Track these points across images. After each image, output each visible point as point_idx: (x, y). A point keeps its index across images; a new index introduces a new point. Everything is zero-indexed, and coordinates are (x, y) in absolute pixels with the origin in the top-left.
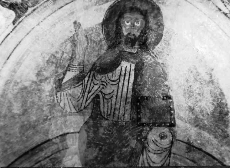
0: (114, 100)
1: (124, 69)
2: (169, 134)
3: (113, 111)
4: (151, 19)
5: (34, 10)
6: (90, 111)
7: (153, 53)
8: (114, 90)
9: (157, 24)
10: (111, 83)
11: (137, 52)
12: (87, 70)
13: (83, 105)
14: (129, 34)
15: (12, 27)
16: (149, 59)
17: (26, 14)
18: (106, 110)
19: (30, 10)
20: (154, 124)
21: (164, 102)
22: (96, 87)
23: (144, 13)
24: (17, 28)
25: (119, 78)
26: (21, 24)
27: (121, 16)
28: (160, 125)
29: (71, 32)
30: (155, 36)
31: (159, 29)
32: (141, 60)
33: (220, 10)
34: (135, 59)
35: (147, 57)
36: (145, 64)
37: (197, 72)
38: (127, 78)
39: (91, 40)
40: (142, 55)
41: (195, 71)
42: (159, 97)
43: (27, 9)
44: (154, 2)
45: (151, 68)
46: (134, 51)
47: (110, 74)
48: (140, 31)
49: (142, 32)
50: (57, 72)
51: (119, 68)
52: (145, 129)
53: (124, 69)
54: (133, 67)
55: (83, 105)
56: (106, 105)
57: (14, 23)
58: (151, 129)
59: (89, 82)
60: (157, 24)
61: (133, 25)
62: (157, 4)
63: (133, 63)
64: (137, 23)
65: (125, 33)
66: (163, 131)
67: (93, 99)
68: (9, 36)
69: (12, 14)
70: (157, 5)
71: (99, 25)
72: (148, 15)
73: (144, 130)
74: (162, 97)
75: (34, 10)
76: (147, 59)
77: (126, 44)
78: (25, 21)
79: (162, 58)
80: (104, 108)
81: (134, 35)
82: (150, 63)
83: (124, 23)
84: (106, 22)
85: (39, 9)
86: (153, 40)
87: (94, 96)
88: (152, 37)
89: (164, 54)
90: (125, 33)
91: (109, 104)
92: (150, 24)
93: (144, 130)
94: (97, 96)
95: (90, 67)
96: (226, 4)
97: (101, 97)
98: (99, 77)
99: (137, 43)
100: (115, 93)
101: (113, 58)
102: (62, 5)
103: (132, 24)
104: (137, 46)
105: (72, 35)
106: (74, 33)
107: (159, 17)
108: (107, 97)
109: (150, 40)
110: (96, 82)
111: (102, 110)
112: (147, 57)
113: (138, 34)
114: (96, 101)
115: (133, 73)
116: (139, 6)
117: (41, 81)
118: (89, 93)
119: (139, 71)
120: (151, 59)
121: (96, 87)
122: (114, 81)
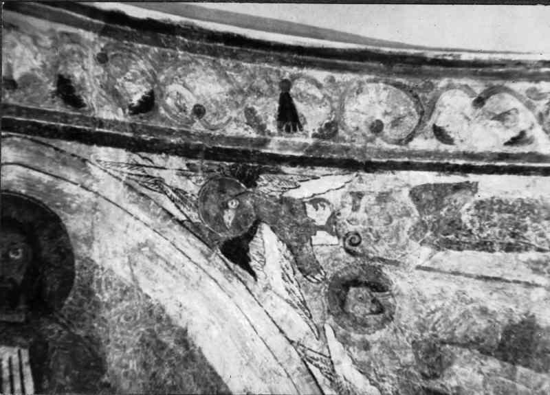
4: (43, 242)
7: (62, 316)
9: (58, 251)
11: (27, 321)
16: (56, 331)
30: (58, 278)
31: (65, 261)
32: (40, 336)
33: (170, 215)
34: (26, 337)
35: (50, 327)
36: (51, 345)
38: (17, 386)
40: (39, 324)
41: (154, 341)
44: (44, 205)
45: (67, 352)
48: (24, 270)
49: (27, 274)
54: (25, 353)
62: (52, 209)
63: (24, 347)
64: (14, 253)
70: (53, 212)
76: (51, 332)
79: (83, 325)
81: (11, 280)
82: (59, 340)
86: (56, 287)
88: (52, 283)
89: (85, 315)
92: (44, 253)
96: (180, 205)
99: (22, 299)
104: (22, 307)
107: (60, 235)
109: (49, 289)
112: (50, 327)
115: (27, 370)
116: (14, 214)
120: (60, 332)
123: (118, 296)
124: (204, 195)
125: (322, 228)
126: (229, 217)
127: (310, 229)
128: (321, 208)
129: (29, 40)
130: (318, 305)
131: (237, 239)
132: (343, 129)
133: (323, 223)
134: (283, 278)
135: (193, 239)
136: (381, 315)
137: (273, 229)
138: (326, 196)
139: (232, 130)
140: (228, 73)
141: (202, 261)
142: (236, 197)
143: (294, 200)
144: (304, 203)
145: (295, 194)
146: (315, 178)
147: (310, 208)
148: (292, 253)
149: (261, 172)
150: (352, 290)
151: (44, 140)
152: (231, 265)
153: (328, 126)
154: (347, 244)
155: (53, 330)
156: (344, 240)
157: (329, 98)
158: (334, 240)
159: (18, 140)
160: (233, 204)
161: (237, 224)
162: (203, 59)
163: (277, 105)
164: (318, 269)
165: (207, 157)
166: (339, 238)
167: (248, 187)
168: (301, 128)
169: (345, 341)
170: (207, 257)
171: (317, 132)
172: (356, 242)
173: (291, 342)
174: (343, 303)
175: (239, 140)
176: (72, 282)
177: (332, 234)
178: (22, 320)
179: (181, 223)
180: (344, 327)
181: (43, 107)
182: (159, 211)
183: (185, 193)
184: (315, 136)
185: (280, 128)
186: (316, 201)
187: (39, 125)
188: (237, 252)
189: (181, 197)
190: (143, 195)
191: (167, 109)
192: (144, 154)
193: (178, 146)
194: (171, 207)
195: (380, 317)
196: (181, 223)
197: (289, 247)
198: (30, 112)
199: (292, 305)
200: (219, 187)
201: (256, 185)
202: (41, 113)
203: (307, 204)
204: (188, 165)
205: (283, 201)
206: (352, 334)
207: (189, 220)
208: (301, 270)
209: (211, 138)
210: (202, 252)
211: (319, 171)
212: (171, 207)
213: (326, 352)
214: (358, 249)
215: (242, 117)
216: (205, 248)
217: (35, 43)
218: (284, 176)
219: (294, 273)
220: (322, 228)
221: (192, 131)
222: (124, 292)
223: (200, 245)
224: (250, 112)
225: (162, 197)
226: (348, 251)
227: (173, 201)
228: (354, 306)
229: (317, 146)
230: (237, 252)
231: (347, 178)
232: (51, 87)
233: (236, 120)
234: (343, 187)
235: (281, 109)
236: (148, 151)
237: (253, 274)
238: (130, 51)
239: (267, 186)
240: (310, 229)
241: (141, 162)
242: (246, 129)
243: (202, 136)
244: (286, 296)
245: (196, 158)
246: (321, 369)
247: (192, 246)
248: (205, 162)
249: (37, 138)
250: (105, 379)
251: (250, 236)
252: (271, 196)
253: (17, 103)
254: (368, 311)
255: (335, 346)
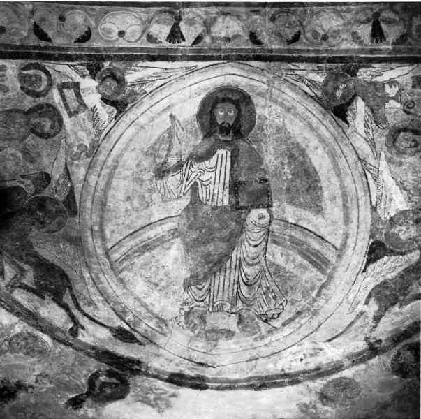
0: (212, 186)
1: (220, 156)
2: (267, 215)
3: (211, 196)
4: (243, 108)
5: (133, 105)
6: (189, 197)
8: (211, 178)
10: (209, 170)
11: (232, 140)
12: (184, 158)
13: (182, 191)
14: (223, 123)
15: (113, 121)
17: (126, 109)
18: (204, 196)
19: (129, 105)
20: (252, 207)
21: (260, 186)
22: (194, 175)
23: (236, 103)
24: (118, 123)
25: (216, 166)
26: (122, 118)
27: (214, 107)
28: (258, 207)
29: (168, 124)
33: (307, 93)
34: (230, 147)
37: (291, 153)
38: (224, 165)
39: (187, 131)
41: (288, 153)
42: (256, 180)
43: (126, 105)
46: (229, 139)
47: (207, 162)
50: (156, 162)
51: (216, 156)
52: (243, 211)
53: (220, 156)
54: (229, 153)
55: (182, 191)
56: (204, 190)
57: (115, 118)
58: (249, 211)
59: (187, 170)
60: (249, 111)
61: (226, 115)
65: (220, 123)
66: (262, 212)
67: (192, 186)
68: (112, 130)
69: (113, 110)
71: (194, 116)
72: (240, 104)
73: (242, 213)
74: (259, 181)
75: (133, 105)
76: (242, 145)
77: (221, 132)
78: (125, 116)
80: (203, 195)
83: (217, 112)
84: (200, 114)
85: (137, 105)
87: (192, 183)
88: (245, 127)
90: (220, 123)
91: (208, 190)
93: (242, 213)
94: (196, 183)
95: (187, 156)
97: (199, 184)
98: (196, 165)
99: (231, 131)
100: (213, 180)
101: (208, 147)
102: (158, 100)
103: (225, 113)
105: (168, 127)
106: (170, 125)
108: (205, 183)
110: (193, 170)
111: (201, 196)
112: (242, 143)
113: (231, 123)
114: (195, 187)
115: (229, 159)
116: (230, 96)
117: (141, 171)
118: (187, 180)
119: (235, 157)
121: (194, 175)
122: (211, 168)
123: (275, 132)
124: (326, 83)
125: (392, 98)
126: (339, 94)
127: (386, 99)
128: (393, 87)
129: (235, 18)
130: (381, 141)
131: (343, 105)
132: (410, 37)
133: (393, 95)
134: (365, 126)
135: (317, 105)
136: (415, 149)
137: (364, 100)
138: (398, 80)
139: (344, 46)
140: (342, 14)
141: (321, 117)
142: (344, 83)
143: (378, 82)
144: (384, 84)
145: (379, 79)
146: (392, 69)
147: (387, 87)
148: (373, 112)
149: (360, 67)
150: (402, 134)
151: (244, 62)
152: (336, 118)
153: (402, 36)
154: (405, 108)
155: (242, 144)
156: (404, 105)
157: (403, 19)
158: (398, 105)
159: (233, 64)
160: (342, 87)
161: (343, 97)
162: (328, 9)
163: (371, 28)
164: (385, 121)
165: (328, 62)
166: (401, 104)
167: (352, 76)
168: (385, 40)
169: (389, 161)
170: (324, 114)
171: (395, 41)
172: (411, 106)
173: (360, 159)
174: (395, 140)
175: (347, 51)
176: (254, 126)
177: (398, 102)
178: (230, 139)
179: (312, 97)
180: (391, 154)
181: (243, 47)
182: (300, 91)
183: (315, 82)
184: (393, 43)
185: (372, 41)
186: (392, 83)
187: (241, 56)
188: (340, 112)
189: (312, 84)
190: (293, 84)
191: (307, 39)
192: (294, 64)
193: (313, 57)
194: (307, 89)
195: (413, 149)
196: (312, 97)
197: (372, 110)
198: (237, 50)
199: (367, 141)
200: (334, 77)
201: (356, 75)
202: (241, 50)
203: (386, 85)
204: (318, 67)
205: (371, 83)
206: (395, 158)
207: (316, 95)
208: (376, 122)
209: (332, 51)
210: (322, 112)
211: (393, 65)
212: (307, 89)
213: (377, 166)
214: (412, 111)
215: (350, 38)
216: (324, 111)
217: (240, 19)
218: (373, 70)
219: (371, 124)
220: (392, 98)
221: (321, 49)
222: (278, 131)
223: (321, 108)
224: (354, 34)
225: (303, 84)
226: (405, 111)
227: (308, 86)
228: (401, 142)
229: (394, 50)
230: (340, 112)
231: (411, 68)
232: (247, 38)
233: (346, 40)
234: (407, 73)
235: (373, 30)
236: (296, 61)
237: (348, 123)
238: (288, 12)
239: (364, 74)
240: (386, 99)
241: (293, 67)
242: (352, 44)
243: (327, 51)
244: (364, 135)
245: (322, 63)
246: (372, 174)
247: (314, 108)
248: (328, 64)
249: (241, 62)
250: (262, 167)
251: (349, 104)
252: (366, 81)
253: (231, 47)
254: (409, 146)
255: (383, 163)
